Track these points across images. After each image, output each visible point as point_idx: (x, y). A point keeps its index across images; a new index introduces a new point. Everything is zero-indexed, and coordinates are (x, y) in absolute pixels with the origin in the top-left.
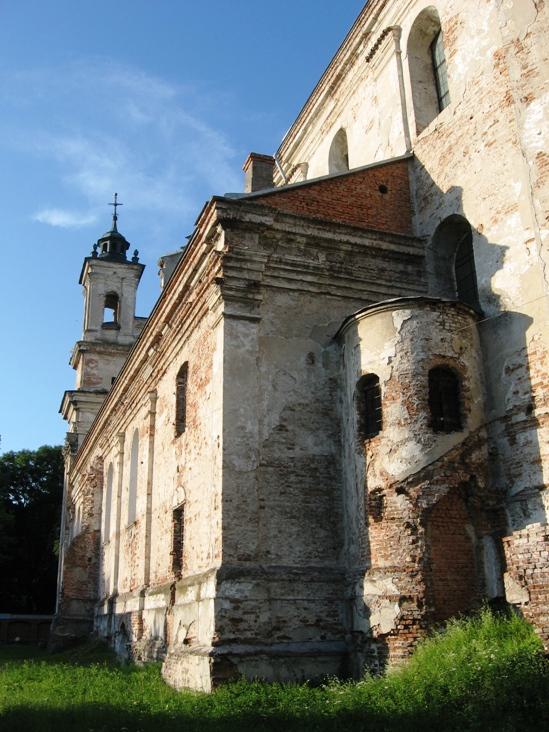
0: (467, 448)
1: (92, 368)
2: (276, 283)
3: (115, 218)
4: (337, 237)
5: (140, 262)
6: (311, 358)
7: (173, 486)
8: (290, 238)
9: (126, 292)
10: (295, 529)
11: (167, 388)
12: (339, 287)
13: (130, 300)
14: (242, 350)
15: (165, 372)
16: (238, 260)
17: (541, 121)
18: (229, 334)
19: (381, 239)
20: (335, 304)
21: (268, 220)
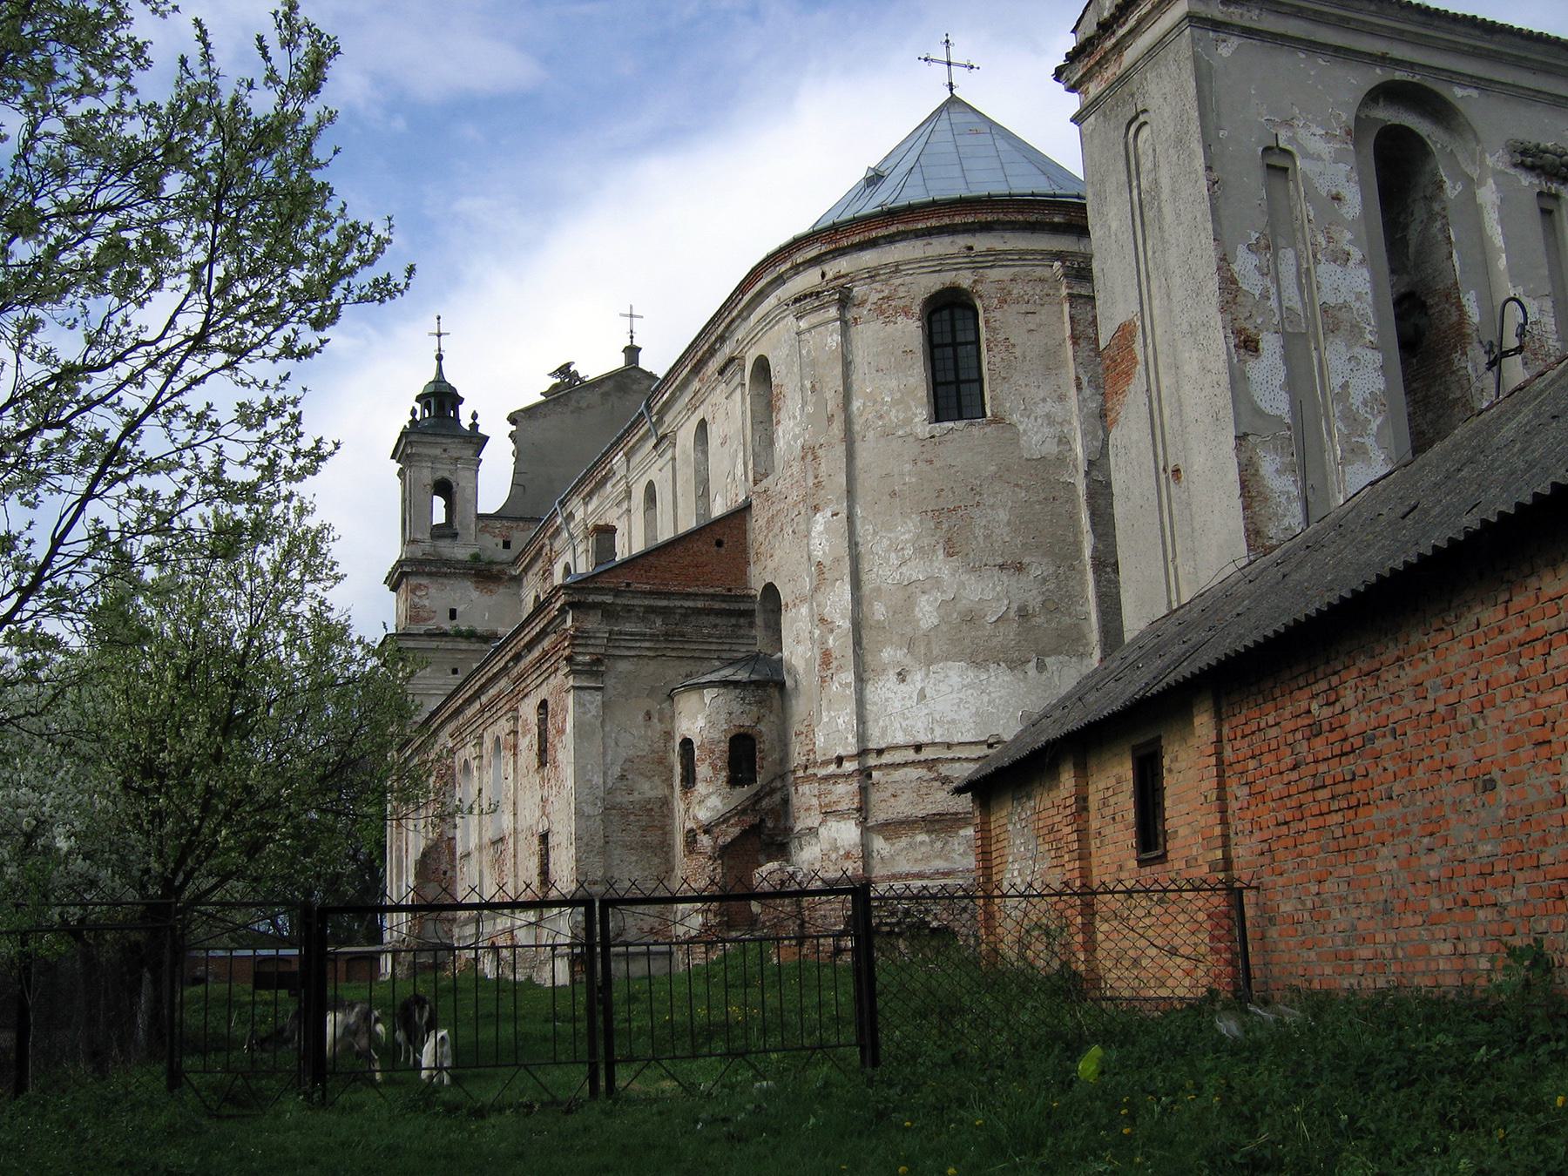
0: (757, 798)
1: (420, 597)
2: (617, 652)
3: (440, 358)
4: (671, 604)
5: (481, 430)
6: (649, 716)
7: (538, 813)
8: (629, 609)
9: (460, 479)
10: (634, 858)
11: (529, 709)
12: (673, 649)
13: (469, 491)
14: (589, 716)
15: (526, 696)
16: (583, 638)
17: (821, 533)
18: (577, 703)
19: (712, 600)
20: (670, 664)
21: (609, 599)
